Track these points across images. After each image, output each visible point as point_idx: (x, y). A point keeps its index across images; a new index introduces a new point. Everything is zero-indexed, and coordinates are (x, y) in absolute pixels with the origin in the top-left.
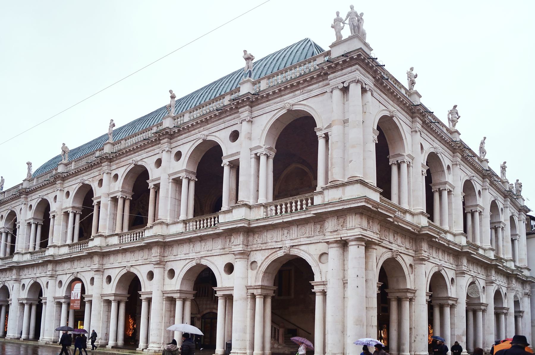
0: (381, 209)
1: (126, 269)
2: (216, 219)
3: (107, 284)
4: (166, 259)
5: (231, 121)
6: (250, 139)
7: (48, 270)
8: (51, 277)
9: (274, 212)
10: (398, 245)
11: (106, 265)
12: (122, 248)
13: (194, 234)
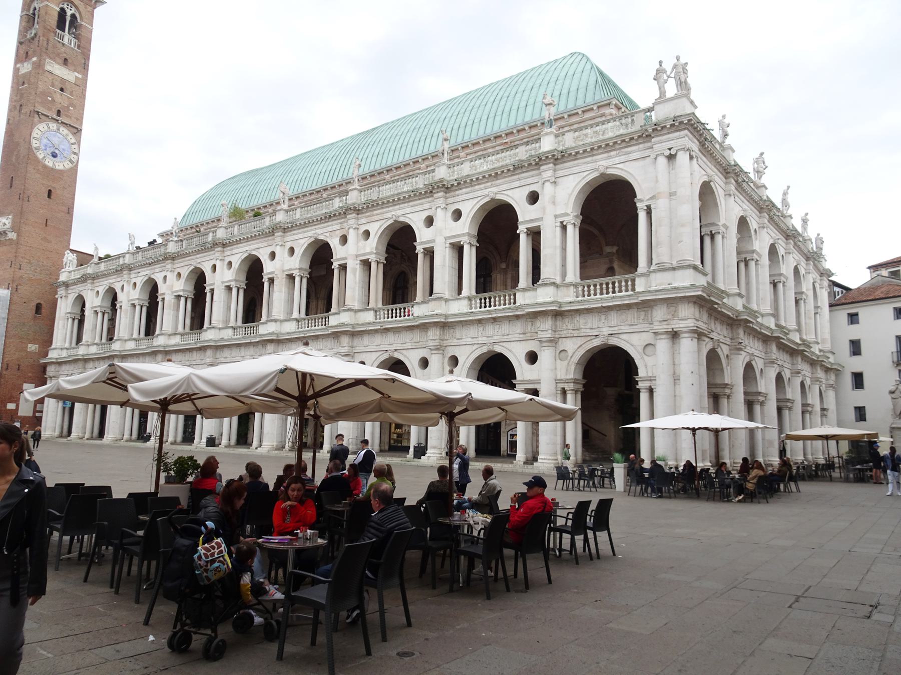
0: (713, 297)
4: (445, 343)
5: (528, 179)
7: (268, 352)
11: (357, 348)
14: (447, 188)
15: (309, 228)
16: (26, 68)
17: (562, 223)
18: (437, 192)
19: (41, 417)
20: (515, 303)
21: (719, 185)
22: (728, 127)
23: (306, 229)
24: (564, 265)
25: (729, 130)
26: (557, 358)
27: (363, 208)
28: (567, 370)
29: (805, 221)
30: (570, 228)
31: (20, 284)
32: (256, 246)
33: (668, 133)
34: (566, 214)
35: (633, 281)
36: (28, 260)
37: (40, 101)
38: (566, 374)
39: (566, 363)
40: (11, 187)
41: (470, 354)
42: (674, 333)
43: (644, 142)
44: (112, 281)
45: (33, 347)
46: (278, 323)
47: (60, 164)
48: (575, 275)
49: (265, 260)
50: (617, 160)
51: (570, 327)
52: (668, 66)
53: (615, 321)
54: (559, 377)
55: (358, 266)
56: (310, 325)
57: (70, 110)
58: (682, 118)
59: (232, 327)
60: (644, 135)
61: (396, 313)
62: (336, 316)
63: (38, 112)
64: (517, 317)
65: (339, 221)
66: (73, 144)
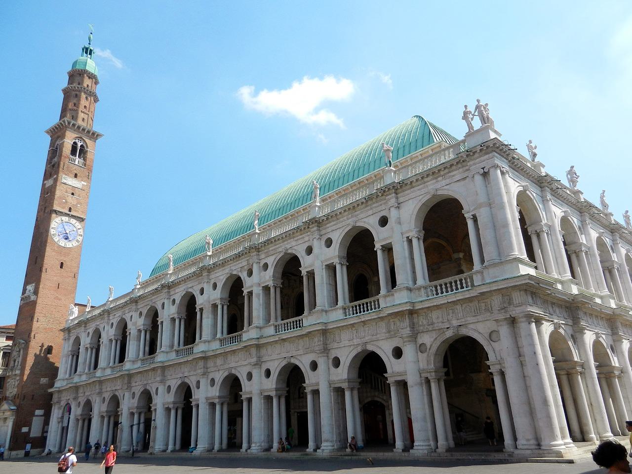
1: (286, 360)
3: (266, 378)
15: (226, 267)
16: (49, 183)
17: (408, 237)
18: (313, 227)
19: (47, 437)
20: (379, 308)
24: (414, 272)
26: (419, 351)
27: (261, 246)
28: (428, 361)
30: (415, 242)
31: (37, 333)
32: (190, 285)
33: (480, 156)
34: (410, 231)
36: (45, 314)
37: (57, 203)
38: (428, 365)
39: (425, 355)
40: (36, 263)
41: (349, 354)
43: (463, 167)
45: (44, 381)
46: (207, 343)
47: (70, 244)
48: (424, 279)
50: (444, 183)
51: (425, 322)
52: (472, 108)
53: (461, 314)
54: (421, 367)
55: (261, 292)
56: (232, 342)
59: (176, 350)
61: (291, 326)
62: (247, 334)
63: (56, 212)
64: (382, 318)
65: (246, 259)
66: (79, 229)
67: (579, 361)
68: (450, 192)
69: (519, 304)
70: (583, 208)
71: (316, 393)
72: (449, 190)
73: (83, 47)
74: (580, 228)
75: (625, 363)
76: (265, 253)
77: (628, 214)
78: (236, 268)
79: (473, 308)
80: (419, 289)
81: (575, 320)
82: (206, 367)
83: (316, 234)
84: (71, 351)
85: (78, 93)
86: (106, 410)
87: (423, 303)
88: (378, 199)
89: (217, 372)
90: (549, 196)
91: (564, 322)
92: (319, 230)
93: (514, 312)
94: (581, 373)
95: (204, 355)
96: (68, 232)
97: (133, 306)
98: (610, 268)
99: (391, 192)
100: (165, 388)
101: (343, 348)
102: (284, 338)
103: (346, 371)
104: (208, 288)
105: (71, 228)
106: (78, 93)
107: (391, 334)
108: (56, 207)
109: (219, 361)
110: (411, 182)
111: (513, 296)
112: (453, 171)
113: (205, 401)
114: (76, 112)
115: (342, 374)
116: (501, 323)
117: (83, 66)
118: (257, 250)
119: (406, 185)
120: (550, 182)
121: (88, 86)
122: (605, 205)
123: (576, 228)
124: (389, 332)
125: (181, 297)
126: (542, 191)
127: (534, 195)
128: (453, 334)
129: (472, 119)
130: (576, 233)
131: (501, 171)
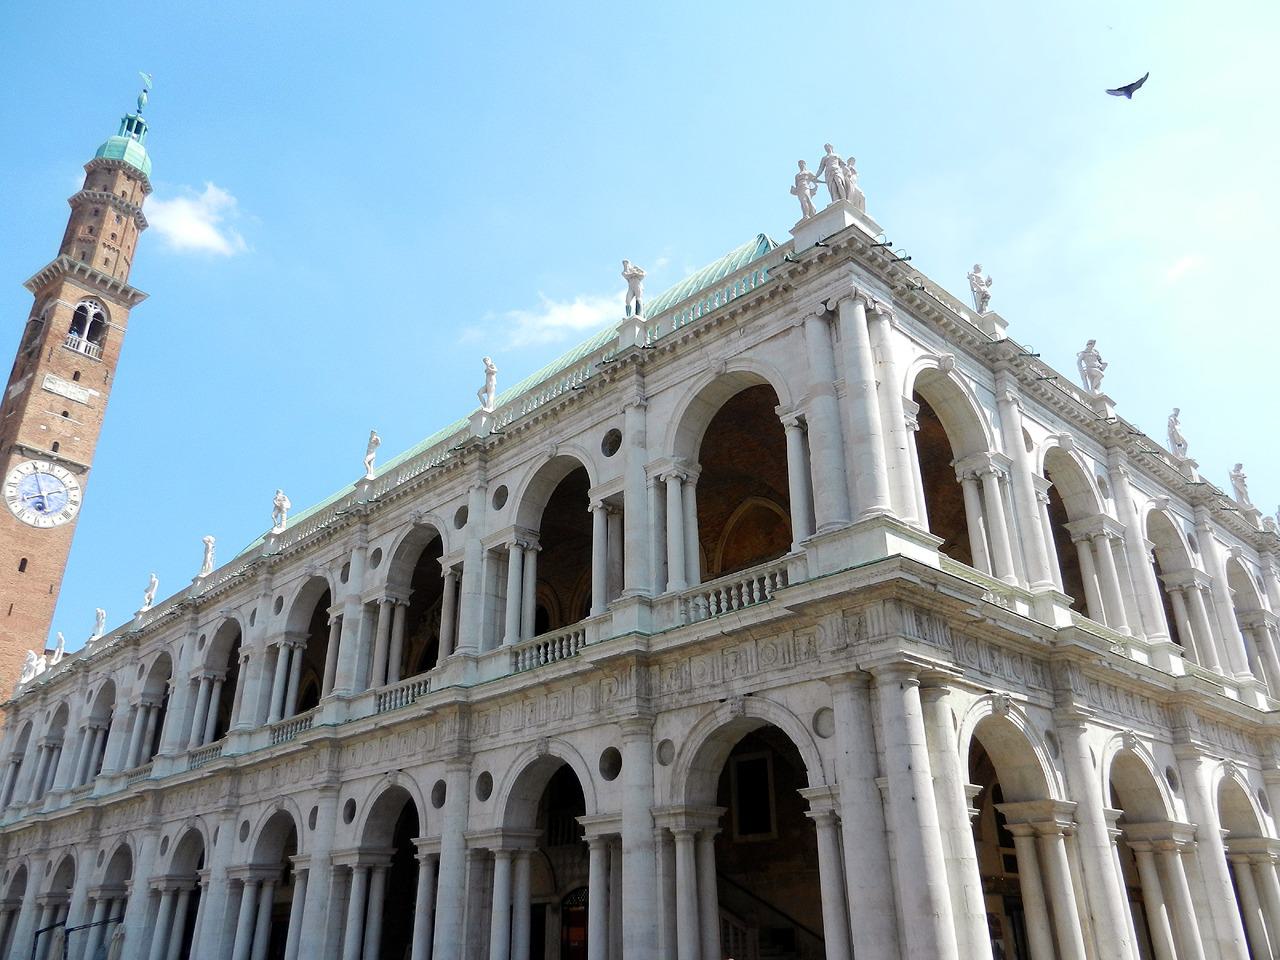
2: (580, 638)
6: (643, 444)
8: (225, 812)
9: (702, 611)
10: (1006, 681)
12: (380, 725)
13: (530, 678)
14: (485, 452)
16: (18, 388)
17: (657, 478)
21: (968, 379)
22: (988, 286)
23: (300, 563)
25: (989, 291)
26: (656, 760)
28: (672, 787)
29: (1239, 479)
30: (673, 488)
32: (235, 604)
33: (820, 275)
34: (662, 461)
35: (784, 574)
38: (672, 796)
39: (669, 768)
41: (511, 767)
42: (864, 677)
43: (785, 303)
44: (67, 692)
46: (245, 738)
48: (687, 579)
49: (245, 627)
50: (742, 344)
51: (675, 689)
52: (812, 168)
54: (658, 803)
55: (361, 615)
57: (74, 441)
58: (835, 239)
60: (781, 289)
63: (21, 449)
65: (343, 540)
67: (1064, 799)
68: (754, 365)
69: (880, 634)
70: (1112, 435)
71: (435, 862)
72: (752, 361)
73: (124, 117)
74: (1101, 483)
75: (1204, 815)
76: (380, 525)
77: (1242, 471)
78: (320, 563)
79: (780, 650)
80: (669, 603)
81: (1060, 695)
82: (235, 794)
83: (476, 477)
84: (14, 754)
85: (99, 206)
86: (48, 891)
87: (669, 636)
88: (605, 390)
89: (256, 807)
90: (1011, 392)
91: (1025, 698)
92: (485, 470)
93: (867, 658)
94: (1067, 834)
95: (230, 765)
96: (44, 494)
97: (129, 653)
98: (1185, 586)
99: (628, 370)
100: (157, 843)
101: (502, 751)
102: (385, 723)
103: (502, 807)
104: (264, 607)
105: (55, 486)
106: (99, 206)
107: (601, 717)
108: (22, 440)
109: (263, 780)
110: (674, 347)
111: (868, 615)
112: (763, 314)
113: (224, 876)
114: (91, 245)
115: (491, 815)
116: (837, 687)
117: (117, 153)
118: (363, 520)
119: (663, 352)
120: (1015, 358)
121: (124, 193)
122: (1178, 443)
123: (1091, 482)
124: (598, 711)
125: (216, 631)
126: (996, 380)
127: (973, 385)
128: (733, 715)
129: (813, 192)
130: (1090, 491)
131: (868, 311)
